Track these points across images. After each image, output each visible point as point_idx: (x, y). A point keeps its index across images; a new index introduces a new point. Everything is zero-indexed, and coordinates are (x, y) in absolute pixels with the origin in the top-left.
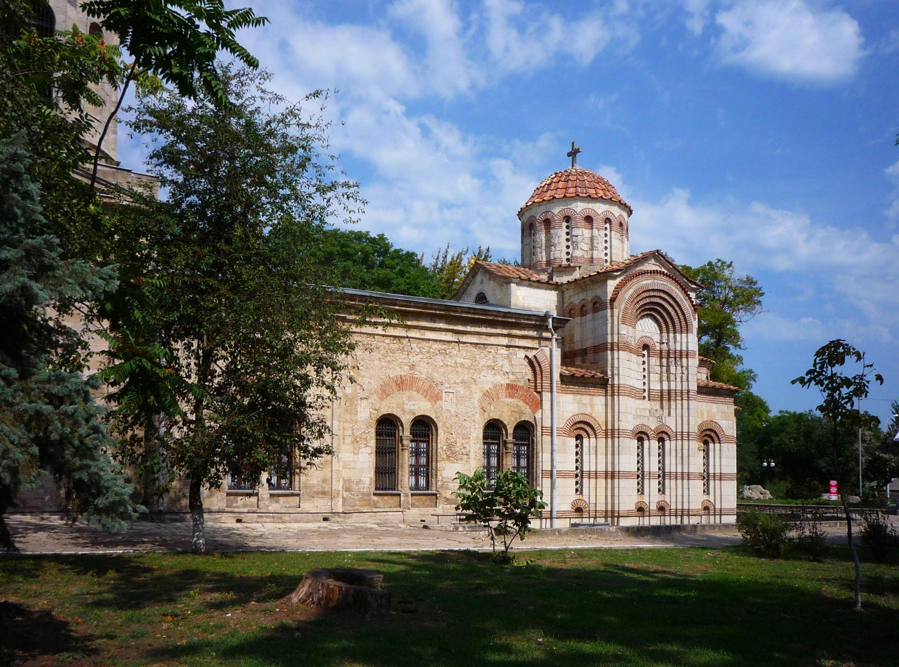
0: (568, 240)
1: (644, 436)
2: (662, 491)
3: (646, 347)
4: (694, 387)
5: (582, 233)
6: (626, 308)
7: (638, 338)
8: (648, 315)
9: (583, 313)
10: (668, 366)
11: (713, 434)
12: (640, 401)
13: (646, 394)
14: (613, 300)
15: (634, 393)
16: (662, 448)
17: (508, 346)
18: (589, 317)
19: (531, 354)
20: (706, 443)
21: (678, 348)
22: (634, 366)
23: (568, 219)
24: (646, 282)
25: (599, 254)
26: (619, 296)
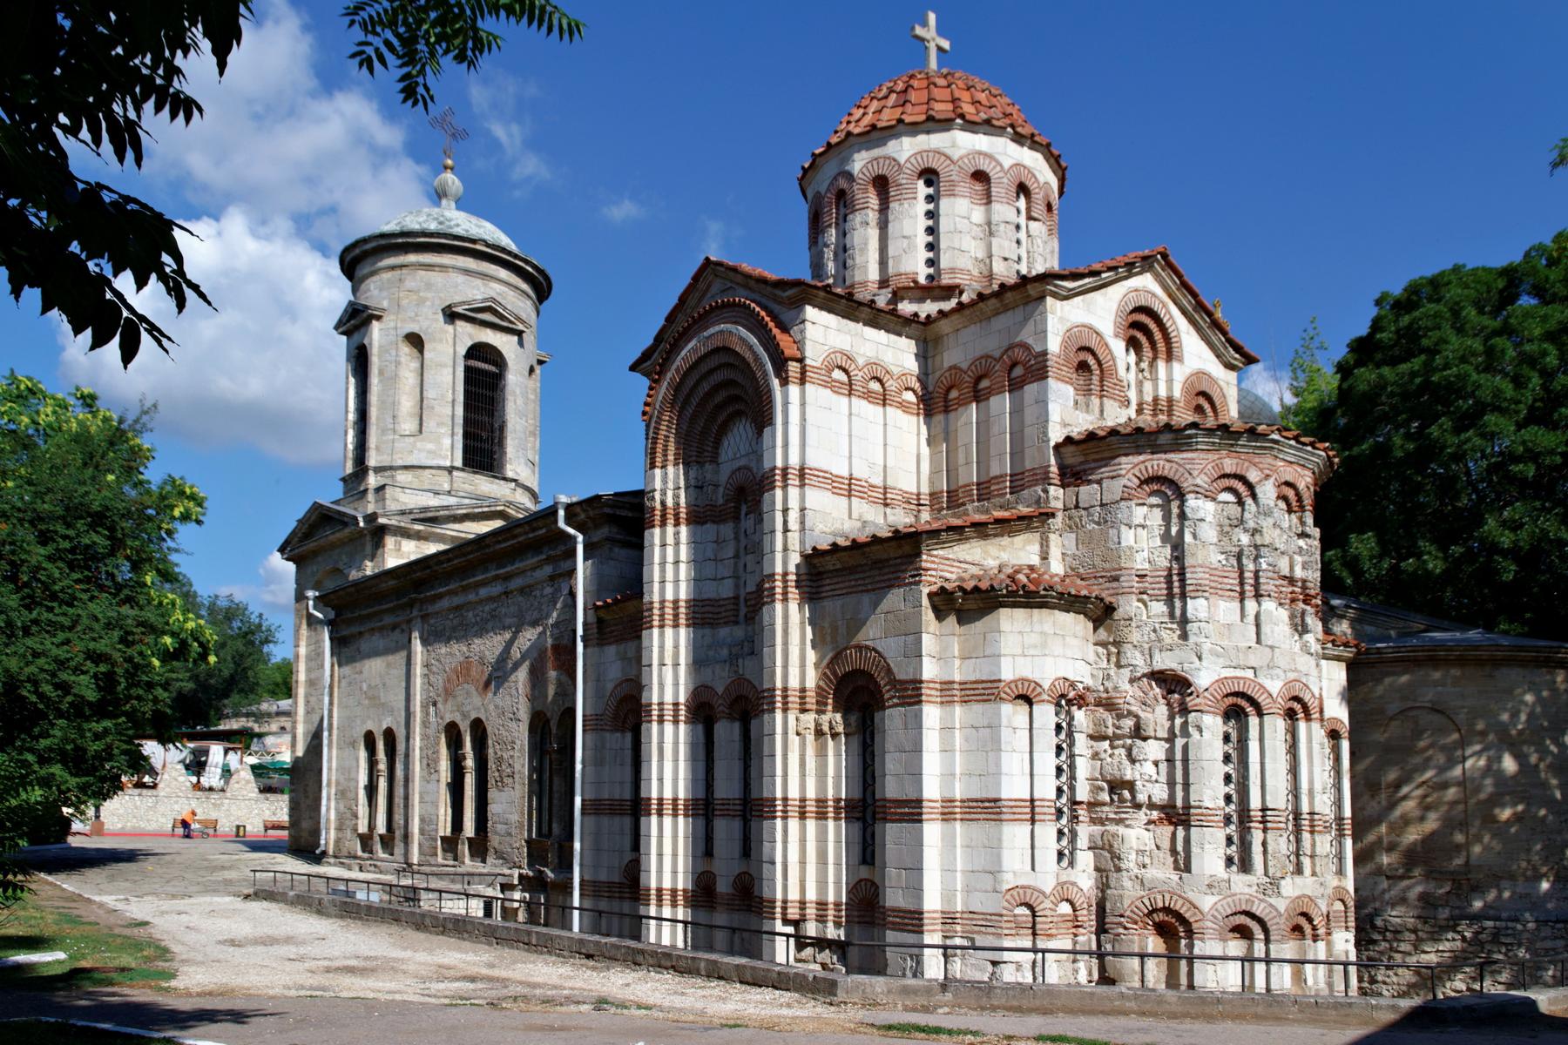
17: (552, 578)
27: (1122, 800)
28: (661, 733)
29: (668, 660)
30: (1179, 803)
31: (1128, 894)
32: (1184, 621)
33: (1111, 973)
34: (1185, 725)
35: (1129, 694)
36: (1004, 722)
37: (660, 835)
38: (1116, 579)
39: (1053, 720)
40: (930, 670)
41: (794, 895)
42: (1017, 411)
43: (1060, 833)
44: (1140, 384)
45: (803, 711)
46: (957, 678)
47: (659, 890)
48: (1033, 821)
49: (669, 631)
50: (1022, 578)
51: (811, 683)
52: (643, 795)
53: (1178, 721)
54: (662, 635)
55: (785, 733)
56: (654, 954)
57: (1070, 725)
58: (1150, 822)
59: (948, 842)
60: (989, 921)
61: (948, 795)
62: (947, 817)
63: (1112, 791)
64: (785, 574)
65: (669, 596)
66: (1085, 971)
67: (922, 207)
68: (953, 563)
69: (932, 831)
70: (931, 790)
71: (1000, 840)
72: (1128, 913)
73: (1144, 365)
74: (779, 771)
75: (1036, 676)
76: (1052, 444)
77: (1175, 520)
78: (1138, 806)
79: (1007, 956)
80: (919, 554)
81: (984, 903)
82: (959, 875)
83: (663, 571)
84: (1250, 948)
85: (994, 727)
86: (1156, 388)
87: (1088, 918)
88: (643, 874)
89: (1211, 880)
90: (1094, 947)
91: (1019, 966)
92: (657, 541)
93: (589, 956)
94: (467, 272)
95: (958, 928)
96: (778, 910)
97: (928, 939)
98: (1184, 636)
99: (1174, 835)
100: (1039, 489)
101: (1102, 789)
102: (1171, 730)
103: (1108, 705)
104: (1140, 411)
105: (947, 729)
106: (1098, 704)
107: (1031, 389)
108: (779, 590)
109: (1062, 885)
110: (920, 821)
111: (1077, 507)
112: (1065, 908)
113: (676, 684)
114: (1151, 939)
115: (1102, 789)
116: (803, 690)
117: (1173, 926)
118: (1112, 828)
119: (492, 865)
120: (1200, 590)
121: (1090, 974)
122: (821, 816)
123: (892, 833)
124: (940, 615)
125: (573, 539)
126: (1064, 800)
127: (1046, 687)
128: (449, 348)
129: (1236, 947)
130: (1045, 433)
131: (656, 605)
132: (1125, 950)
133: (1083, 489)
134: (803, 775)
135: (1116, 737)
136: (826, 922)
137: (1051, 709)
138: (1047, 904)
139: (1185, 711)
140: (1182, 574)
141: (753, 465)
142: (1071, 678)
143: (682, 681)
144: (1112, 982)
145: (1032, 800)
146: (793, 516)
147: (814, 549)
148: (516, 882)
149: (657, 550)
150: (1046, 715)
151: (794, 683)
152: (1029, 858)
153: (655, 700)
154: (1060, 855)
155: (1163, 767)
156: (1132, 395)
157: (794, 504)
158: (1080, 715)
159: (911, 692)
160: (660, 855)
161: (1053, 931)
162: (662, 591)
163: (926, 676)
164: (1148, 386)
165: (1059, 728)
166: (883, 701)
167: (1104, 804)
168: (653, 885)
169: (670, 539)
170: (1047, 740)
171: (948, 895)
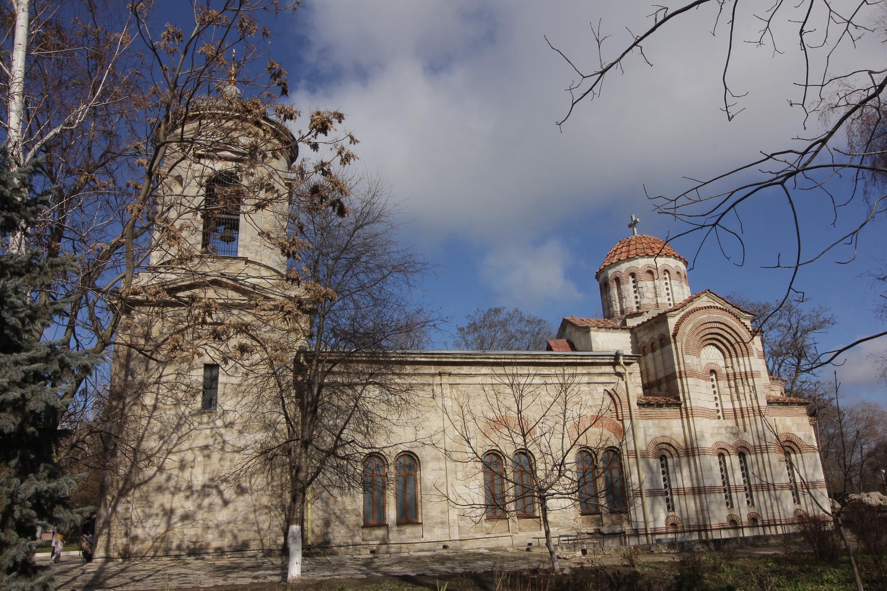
0: (635, 292)
2: (750, 503)
3: (713, 371)
4: (763, 403)
5: (646, 285)
6: (688, 341)
7: (704, 365)
8: (709, 344)
9: (653, 350)
10: (736, 387)
11: (792, 445)
12: (716, 421)
13: (720, 414)
14: (674, 335)
15: (706, 414)
18: (658, 352)
19: (609, 388)
20: (787, 454)
21: (743, 370)
22: (704, 390)
23: (633, 275)
24: (703, 317)
25: (663, 300)
26: (680, 331)
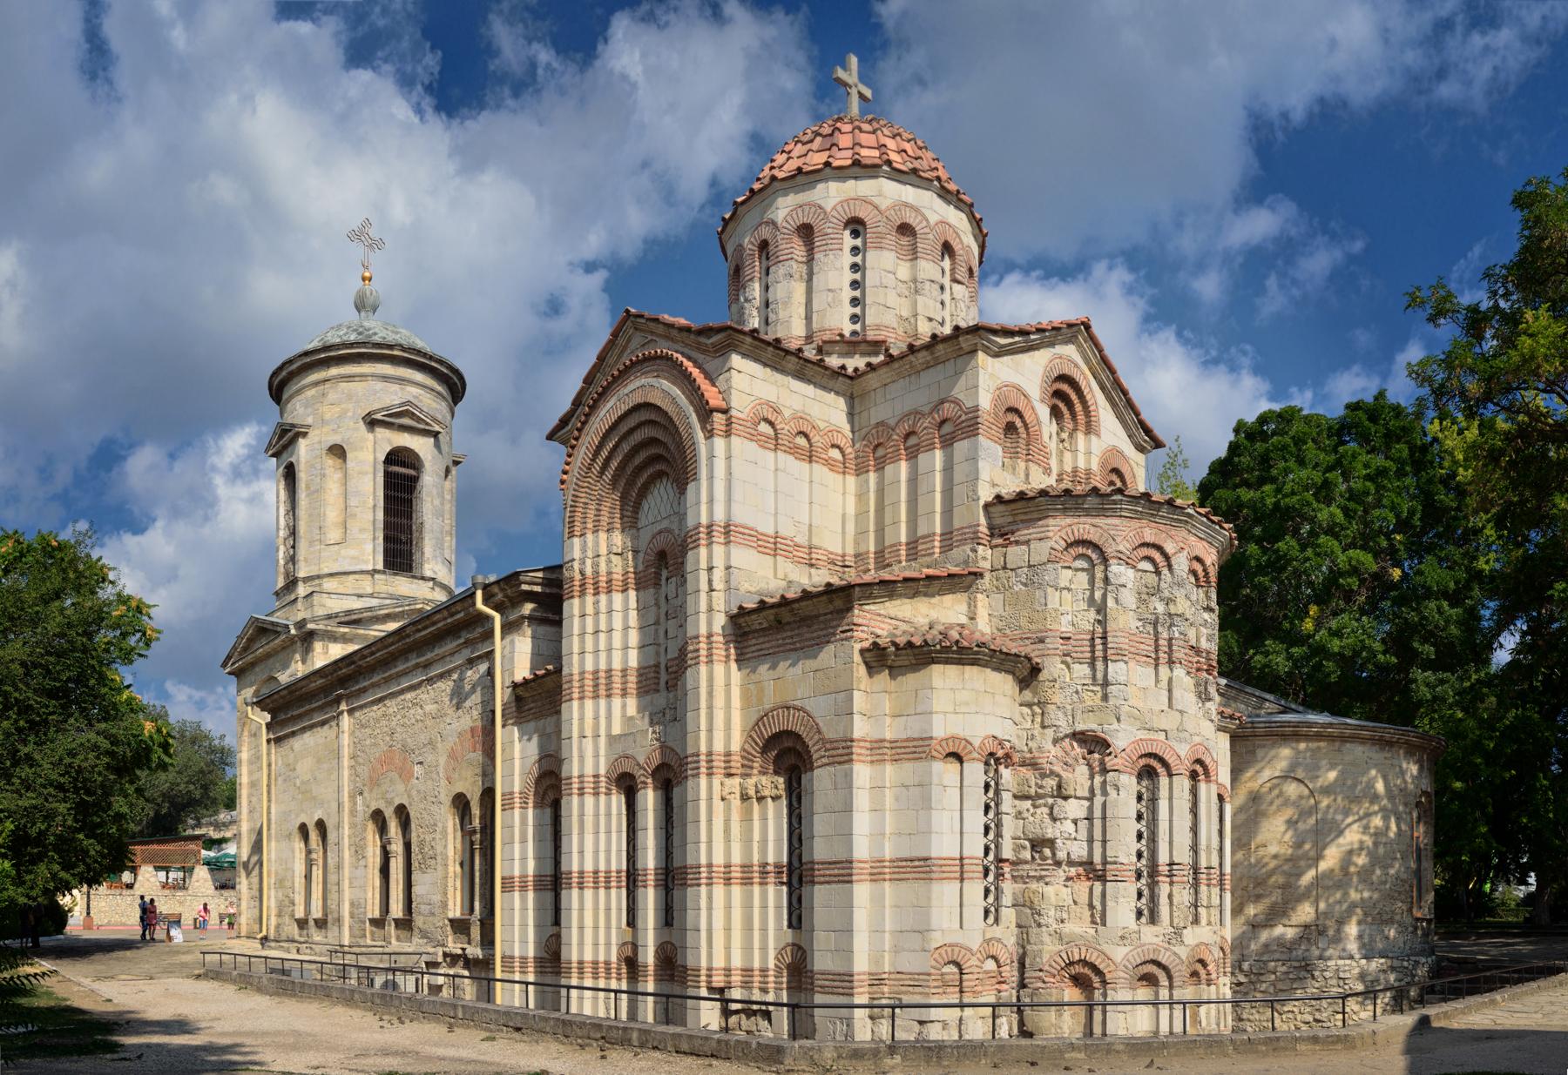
1: (1161, 770)
16: (1194, 792)
27: (1044, 858)
28: (582, 806)
29: (589, 732)
30: (1097, 859)
31: (1048, 951)
32: (1106, 684)
33: (1029, 1027)
34: (1104, 783)
35: (1051, 753)
36: (935, 780)
37: (581, 909)
38: (1042, 641)
39: (981, 779)
40: (861, 728)
41: (719, 962)
42: (948, 469)
43: (987, 892)
44: (1061, 453)
45: (730, 775)
46: (888, 736)
47: (581, 962)
48: (962, 880)
49: (589, 703)
50: (954, 635)
51: (736, 747)
52: (564, 868)
53: (1098, 779)
54: (582, 707)
55: (710, 799)
56: (582, 1025)
57: (997, 784)
58: (1069, 879)
59: (878, 901)
60: (917, 980)
61: (877, 855)
62: (876, 877)
63: (1033, 847)
64: (710, 636)
65: (589, 667)
66: (1007, 1025)
67: (848, 259)
68: (881, 620)
69: (862, 892)
70: (862, 850)
71: (929, 899)
72: (1047, 968)
73: (1065, 435)
74: (703, 837)
75: (966, 734)
76: (982, 503)
77: (1099, 583)
78: (1058, 864)
79: (934, 1014)
80: (850, 609)
81: (912, 963)
82: (887, 935)
83: (582, 642)
84: (1157, 994)
85: (924, 785)
86: (1075, 459)
87: (1011, 973)
88: (563, 948)
89: (1123, 937)
90: (1014, 1000)
91: (945, 1025)
92: (576, 611)
93: (518, 1029)
94: (386, 378)
95: (886, 989)
96: (703, 978)
97: (857, 1000)
98: (1105, 698)
99: (1091, 890)
100: (967, 548)
101: (1024, 848)
102: (1092, 790)
103: (1033, 765)
104: (1059, 480)
105: (877, 788)
106: (1023, 764)
107: (961, 447)
108: (703, 652)
109: (988, 941)
110: (851, 882)
111: (1005, 568)
112: (990, 965)
113: (596, 756)
114: (1067, 992)
115: (1024, 848)
116: (728, 754)
117: (1086, 977)
118: (1034, 886)
119: (415, 944)
120: (1121, 655)
121: (1011, 1029)
122: (747, 881)
123: (821, 896)
124: (871, 669)
125: (489, 618)
126: (991, 857)
127: (977, 743)
128: (370, 450)
129: (1143, 993)
130: (975, 491)
131: (576, 677)
132: (1043, 1000)
133: (1012, 550)
134: (728, 839)
135: (1039, 796)
136: (751, 988)
137: (981, 766)
138: (974, 961)
139: (1104, 771)
140: (1104, 638)
141: (675, 527)
142: (1000, 736)
143: (602, 752)
144: (1030, 1035)
145: (961, 859)
146: (718, 575)
147: (741, 608)
148: (440, 959)
149: (576, 621)
150: (976, 773)
151: (719, 747)
152: (958, 916)
153: (575, 773)
154: (987, 912)
155: (1083, 825)
156: (1054, 463)
157: (719, 562)
158: (1006, 773)
159: (842, 751)
160: (581, 928)
161: (979, 988)
162: (582, 662)
163: (857, 733)
164: (1068, 456)
165: (987, 787)
166: (812, 763)
167: (1026, 862)
168: (575, 958)
169: (590, 609)
170: (977, 798)
171: (876, 958)
